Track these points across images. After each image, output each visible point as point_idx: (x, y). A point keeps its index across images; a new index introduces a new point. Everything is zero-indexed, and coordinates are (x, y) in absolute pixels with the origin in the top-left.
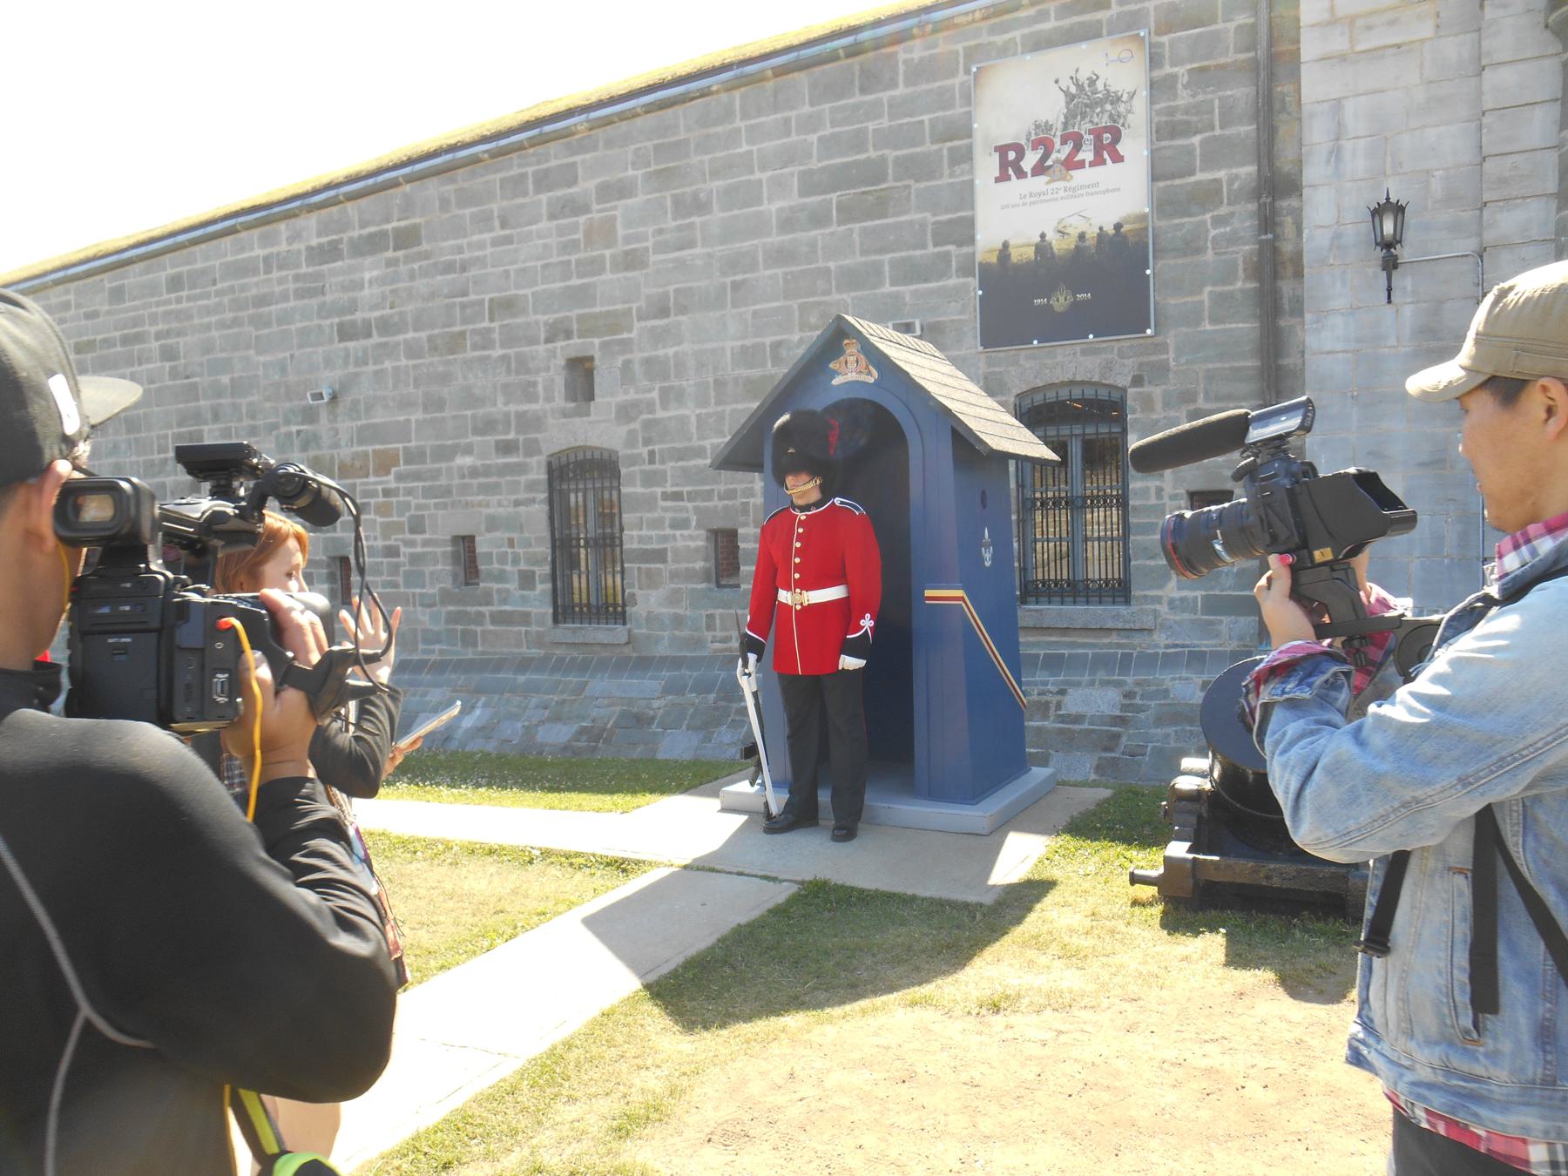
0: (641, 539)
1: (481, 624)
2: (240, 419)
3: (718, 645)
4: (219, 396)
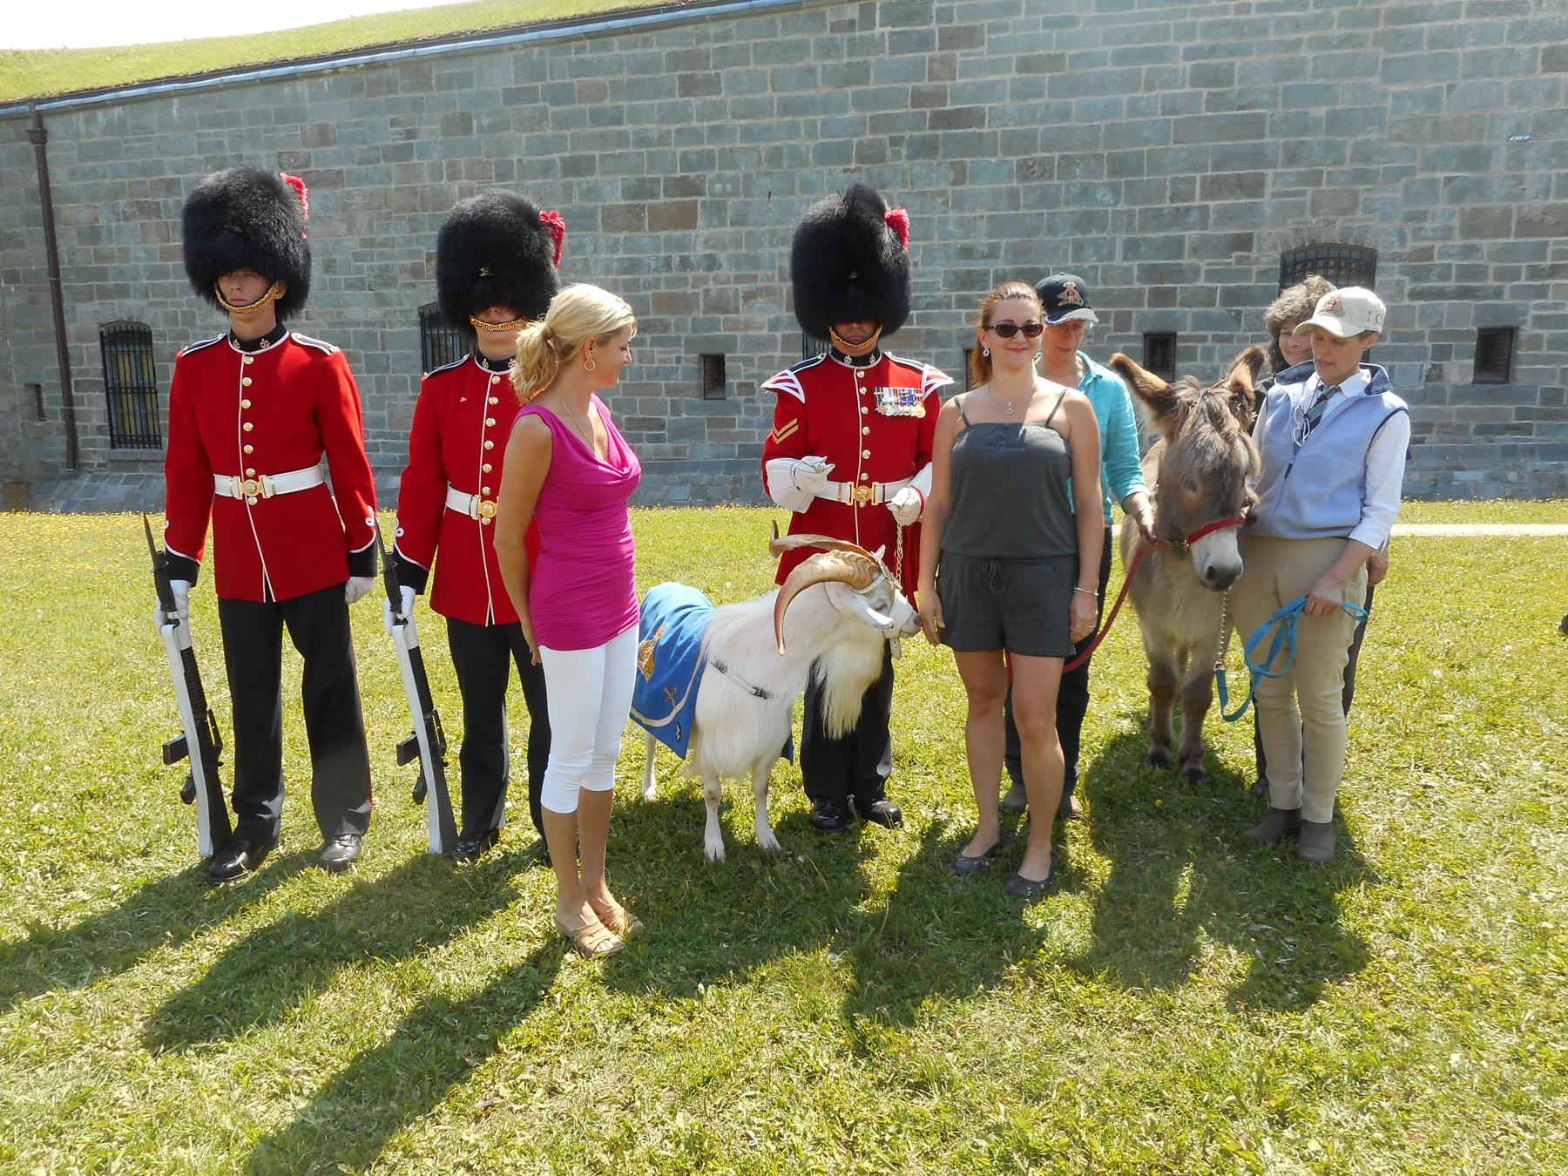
2: (1341, 162)
4: (1304, 130)
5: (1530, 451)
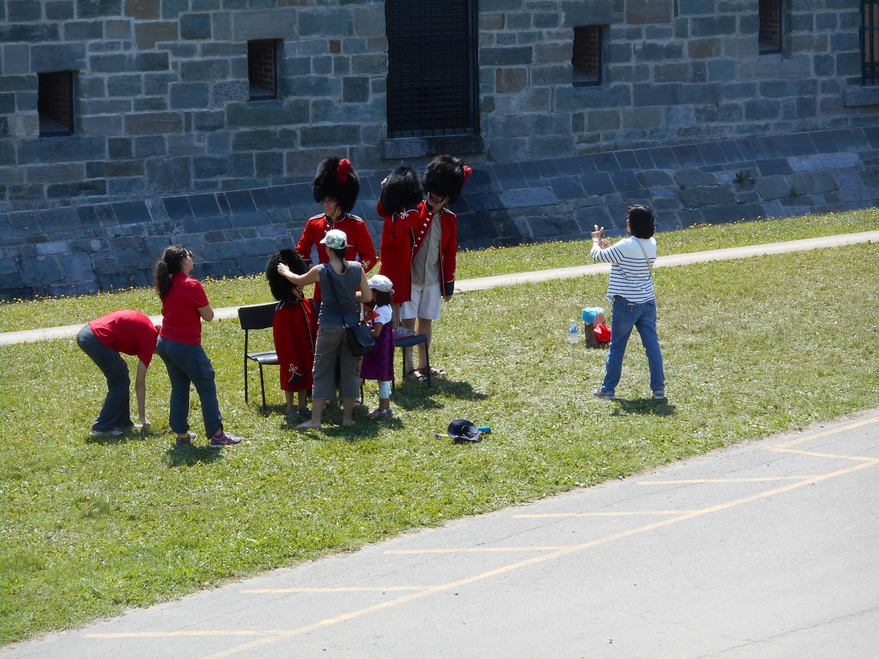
0: (501, 39)
1: (291, 145)
3: (584, 146)
5: (106, 213)
